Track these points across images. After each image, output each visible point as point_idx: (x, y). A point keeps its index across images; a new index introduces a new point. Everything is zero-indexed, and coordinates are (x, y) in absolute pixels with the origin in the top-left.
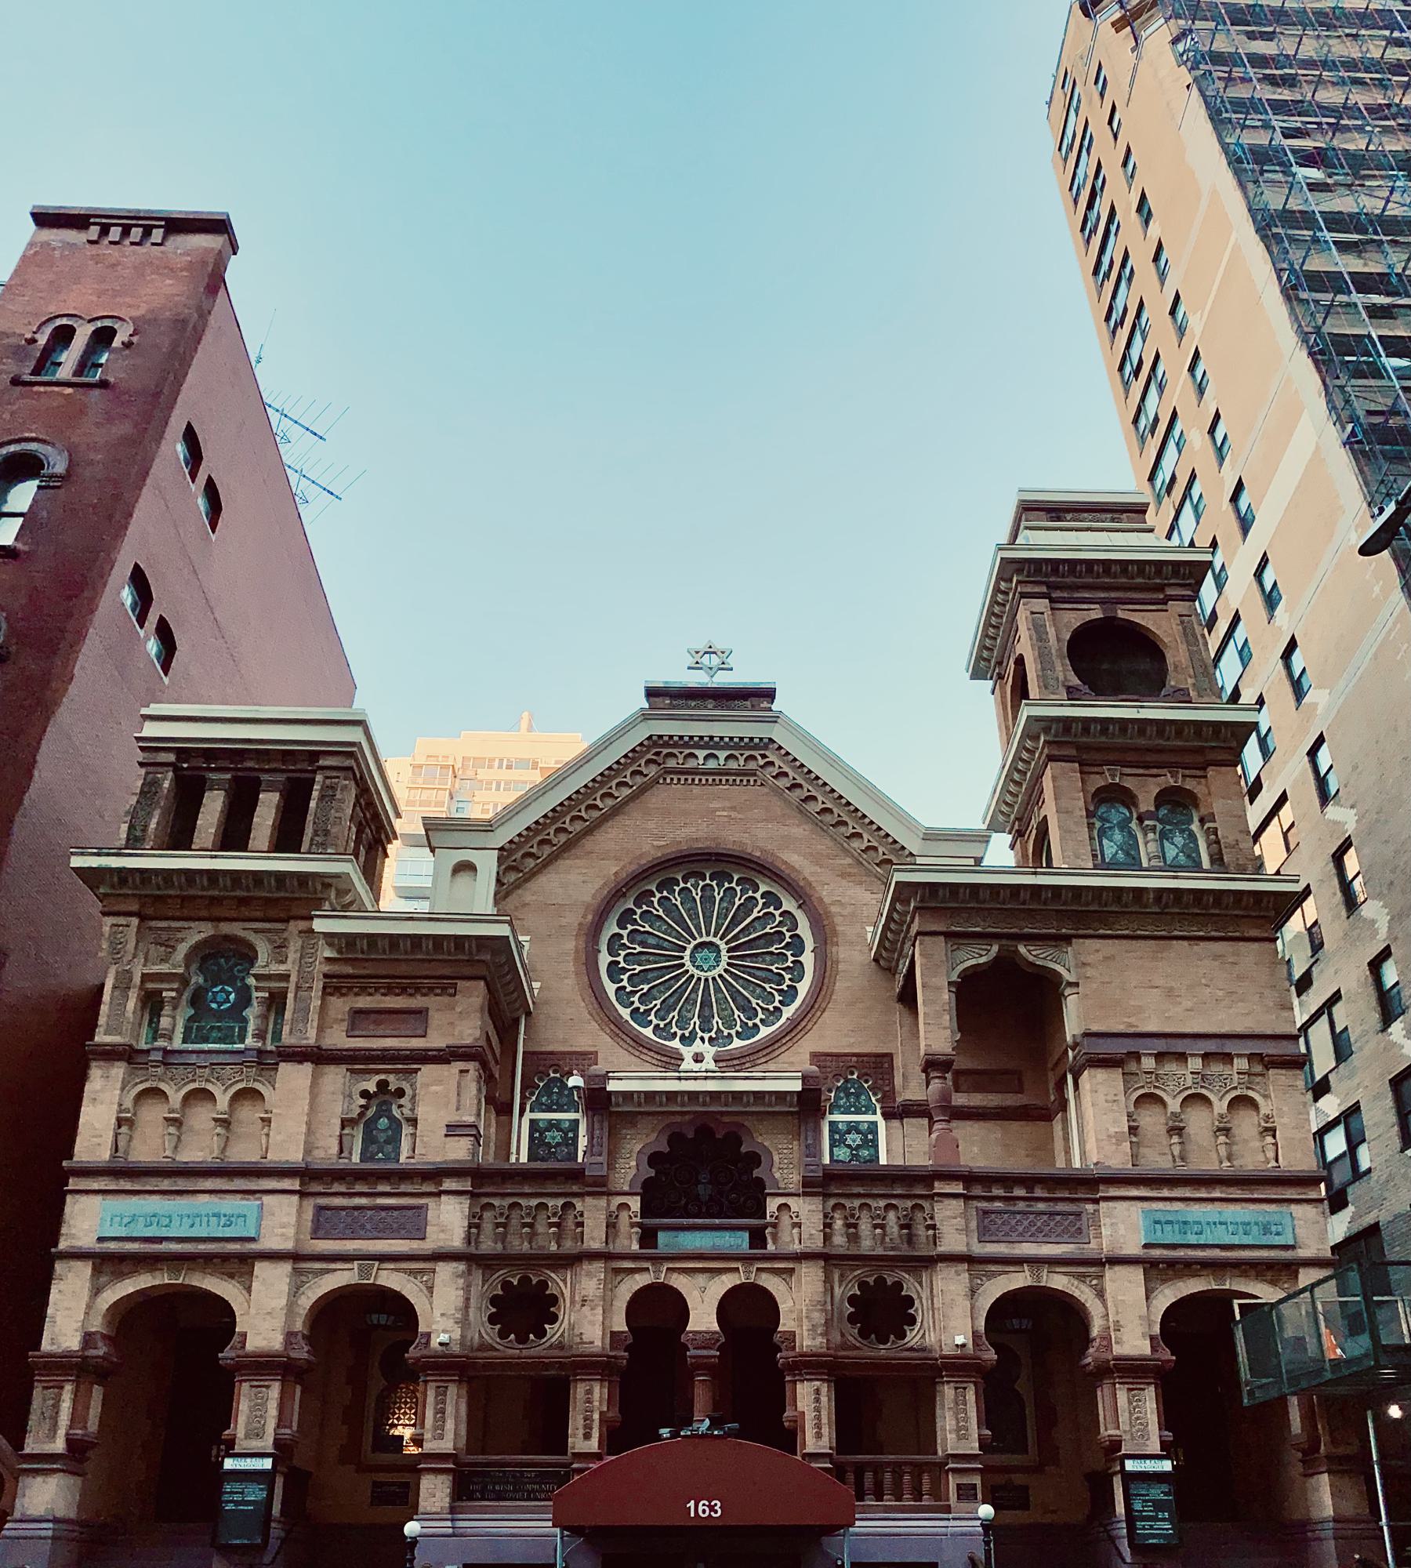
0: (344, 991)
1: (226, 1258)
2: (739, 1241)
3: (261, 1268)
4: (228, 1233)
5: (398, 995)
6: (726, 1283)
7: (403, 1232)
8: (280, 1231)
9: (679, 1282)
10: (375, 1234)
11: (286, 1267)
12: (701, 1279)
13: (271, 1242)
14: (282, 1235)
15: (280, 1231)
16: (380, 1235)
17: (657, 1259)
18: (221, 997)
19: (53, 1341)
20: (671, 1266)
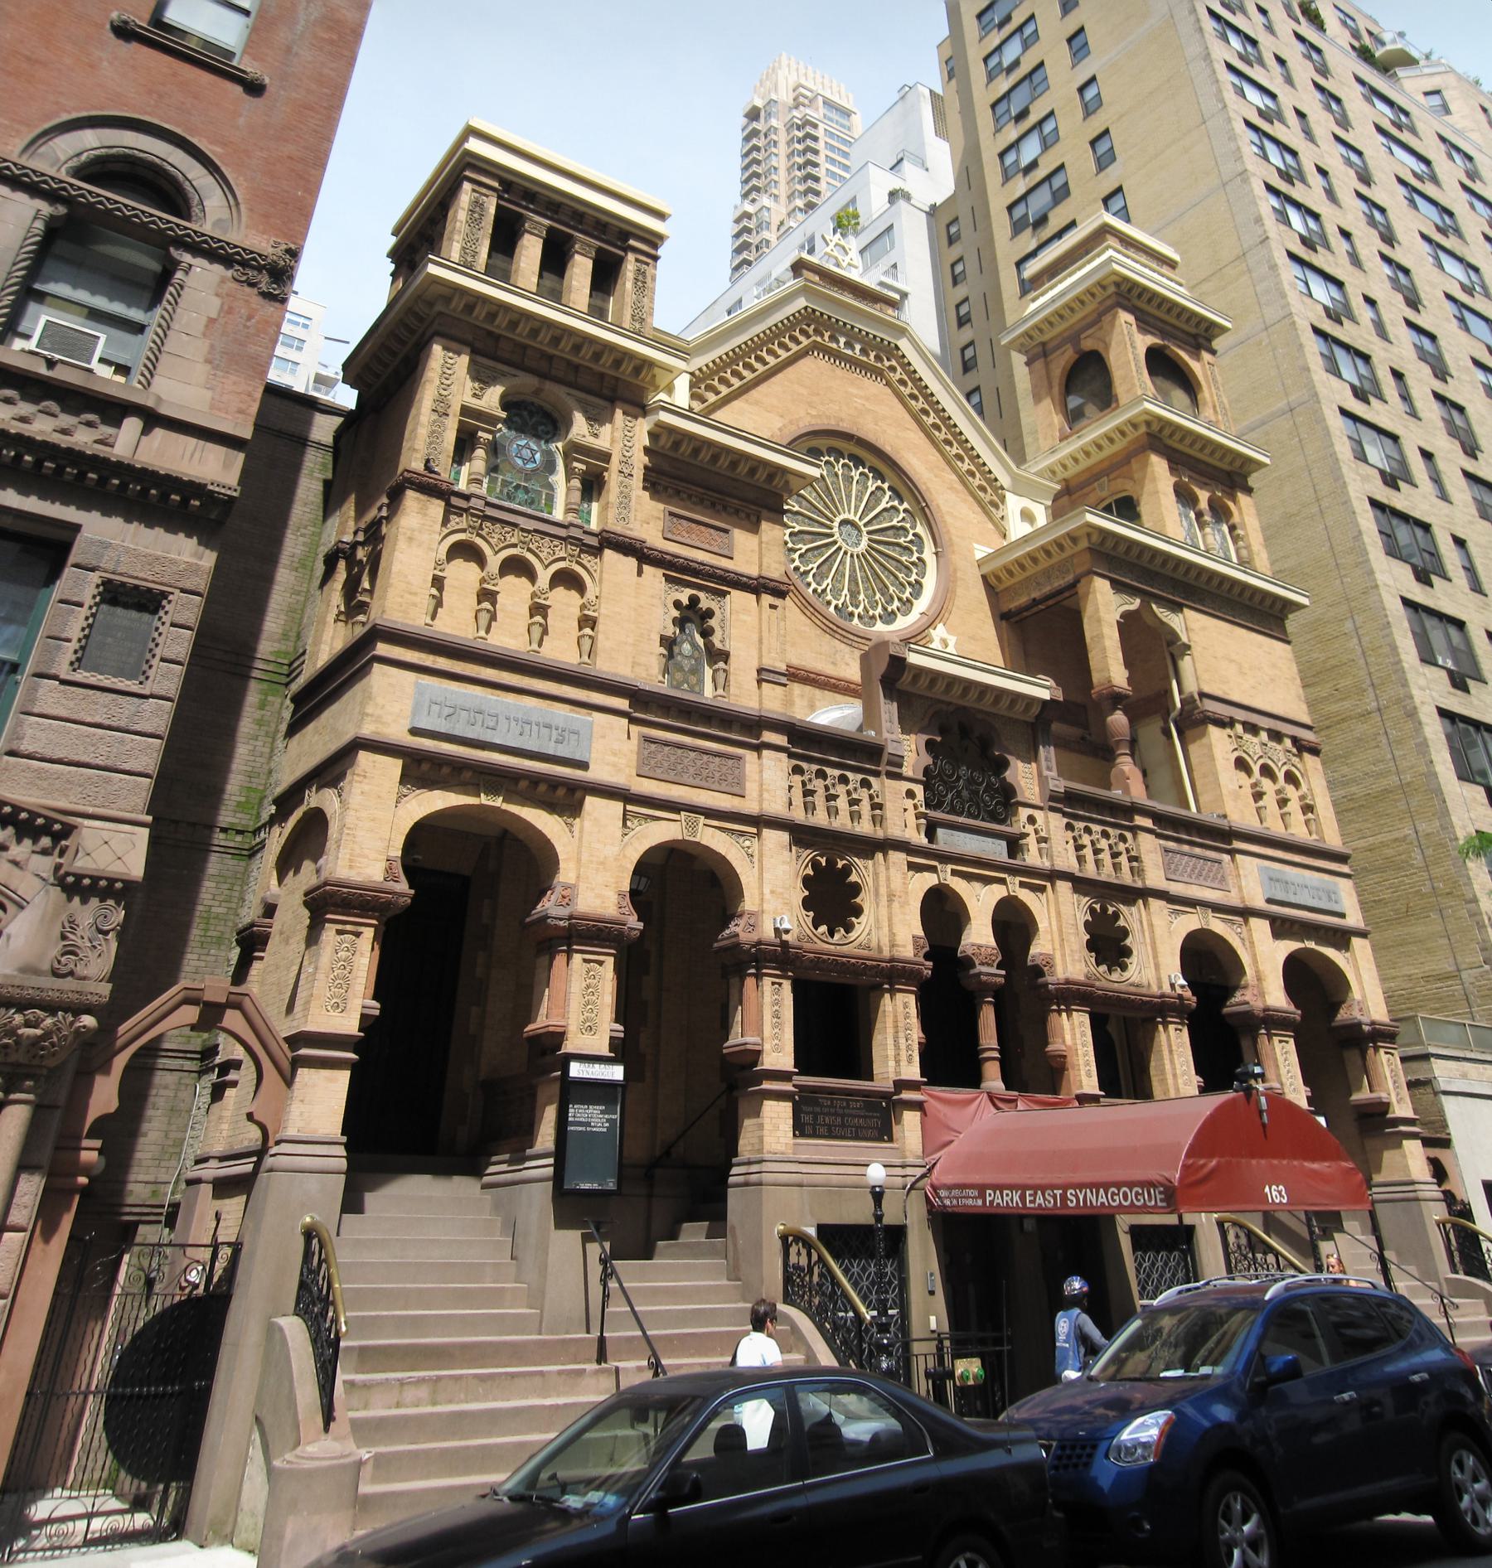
0: (660, 488)
1: (554, 783)
2: (996, 850)
3: (591, 802)
4: (562, 751)
5: (706, 507)
6: (997, 892)
7: (672, 773)
8: (613, 759)
9: (959, 885)
10: (697, 782)
11: (618, 806)
12: (977, 885)
13: (598, 773)
14: (614, 765)
15: (613, 759)
16: (703, 784)
17: (945, 858)
18: (526, 453)
19: (566, 900)
20: (955, 867)
